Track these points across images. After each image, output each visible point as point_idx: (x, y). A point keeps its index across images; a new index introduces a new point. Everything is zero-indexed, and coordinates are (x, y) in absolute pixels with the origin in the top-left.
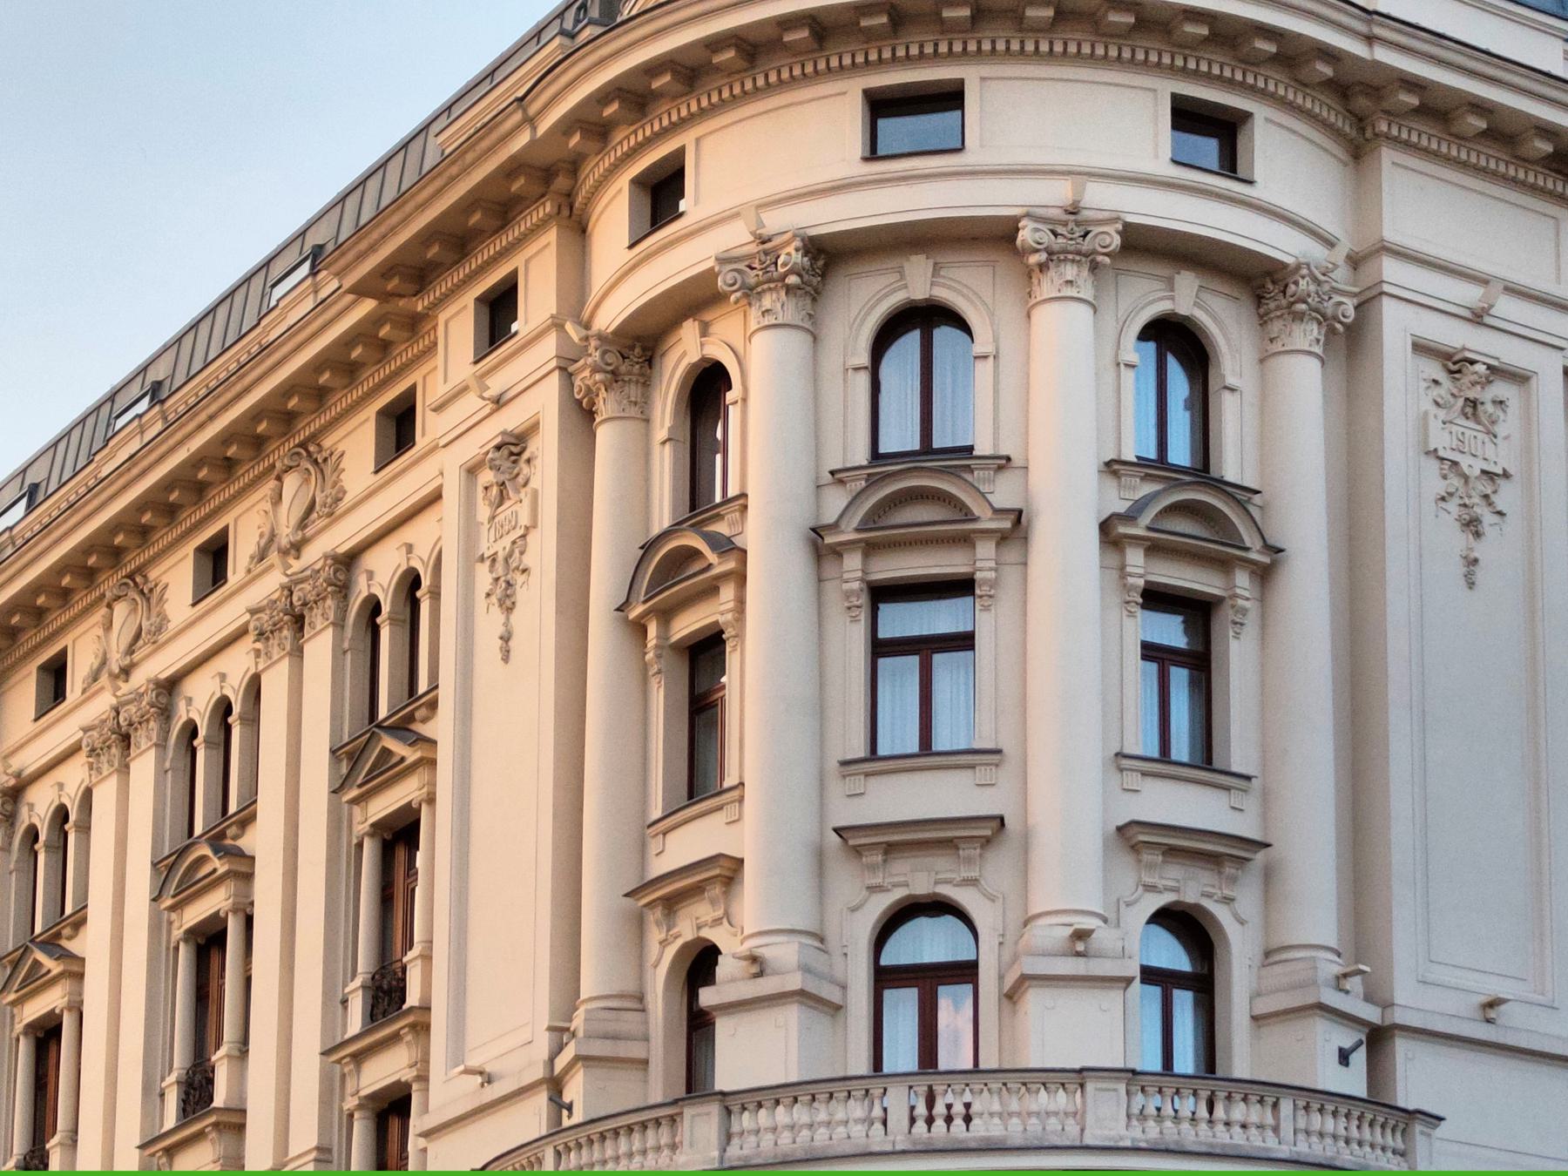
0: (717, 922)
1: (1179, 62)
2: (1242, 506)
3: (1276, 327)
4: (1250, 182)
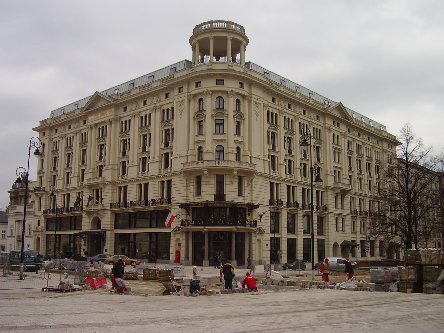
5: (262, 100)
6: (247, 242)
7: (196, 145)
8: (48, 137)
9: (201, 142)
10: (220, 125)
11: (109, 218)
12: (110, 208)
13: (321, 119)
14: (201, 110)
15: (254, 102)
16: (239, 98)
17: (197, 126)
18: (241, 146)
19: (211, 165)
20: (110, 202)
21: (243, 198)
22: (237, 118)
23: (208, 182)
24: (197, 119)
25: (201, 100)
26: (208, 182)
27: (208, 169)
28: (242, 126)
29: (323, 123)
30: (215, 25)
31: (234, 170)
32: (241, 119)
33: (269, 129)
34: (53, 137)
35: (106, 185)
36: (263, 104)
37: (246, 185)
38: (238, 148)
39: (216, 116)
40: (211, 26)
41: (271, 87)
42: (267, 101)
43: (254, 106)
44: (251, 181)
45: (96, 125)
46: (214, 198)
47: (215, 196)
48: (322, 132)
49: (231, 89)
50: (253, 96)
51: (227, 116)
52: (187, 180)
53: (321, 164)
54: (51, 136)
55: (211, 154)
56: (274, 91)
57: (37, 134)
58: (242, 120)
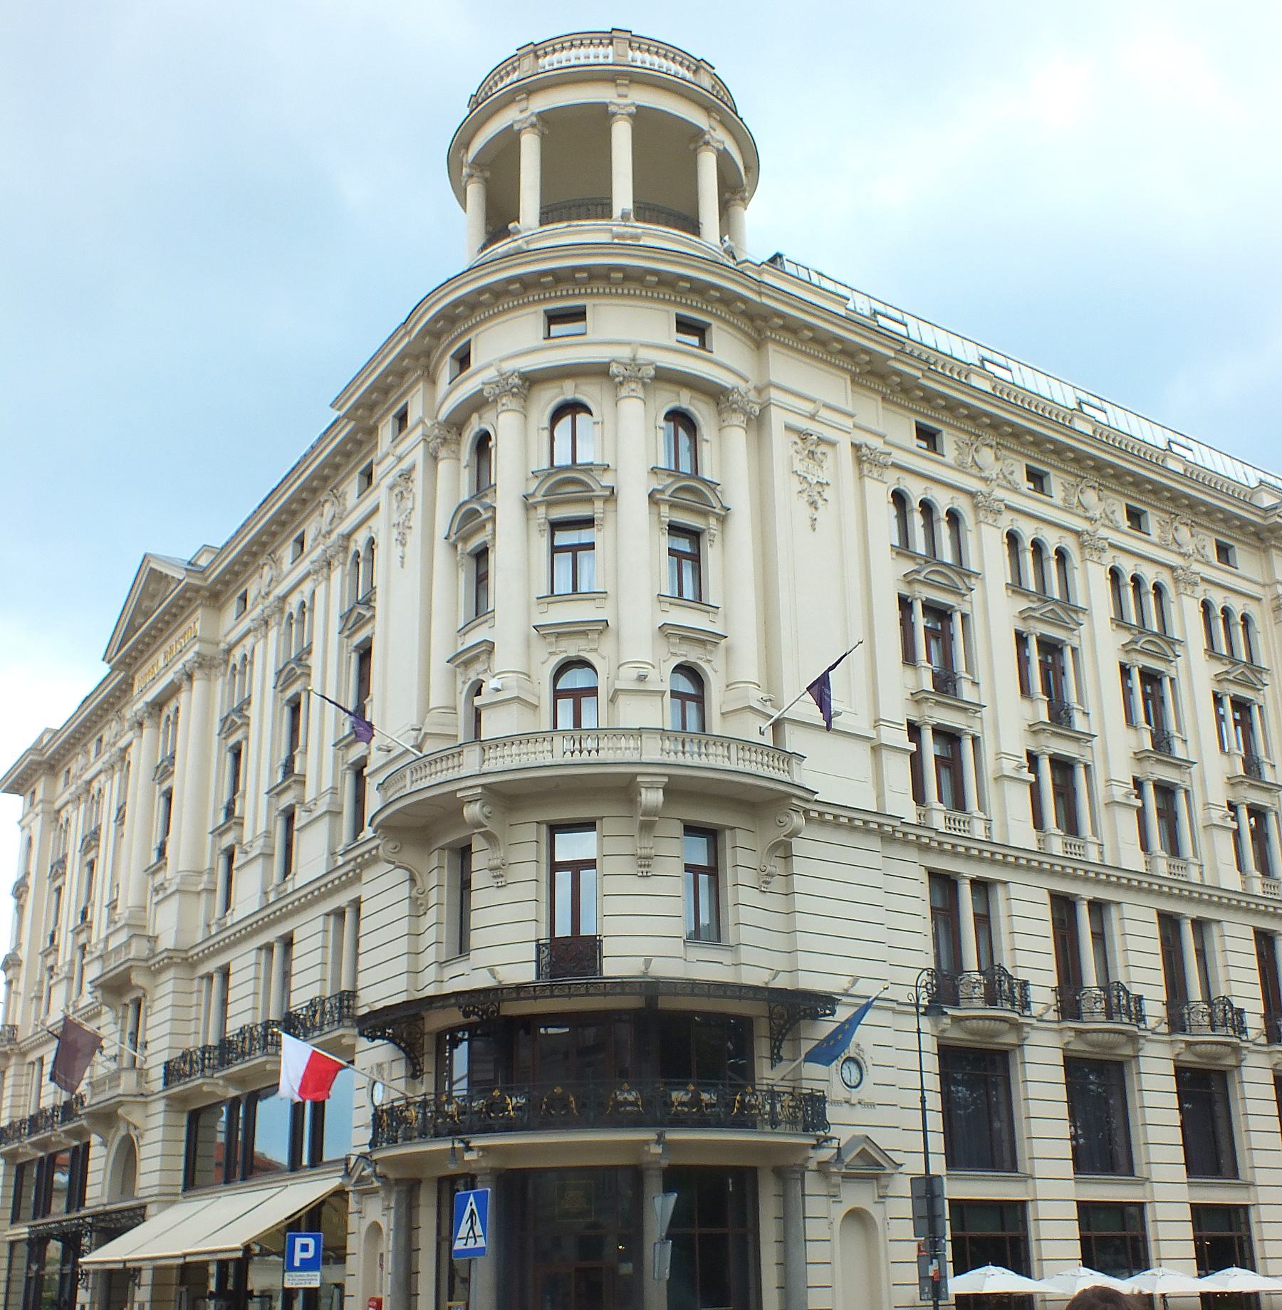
0: (485, 671)
1: (678, 299)
2: (713, 490)
3: (725, 415)
4: (711, 352)
5: (848, 423)
6: (769, 1231)
7: (460, 679)
8: (39, 808)
9: (476, 658)
10: (580, 554)
11: (158, 1134)
12: (158, 1085)
13: (1241, 555)
15: (788, 428)
16: (685, 400)
17: (464, 578)
18: (709, 661)
19: (500, 767)
20: (165, 1057)
21: (726, 957)
22: (673, 506)
23: (497, 871)
24: (465, 539)
25: (483, 443)
26: (497, 871)
27: (483, 786)
28: (711, 555)
29: (1260, 580)
31: (639, 779)
32: (705, 514)
33: (909, 583)
34: (57, 805)
35: (160, 971)
36: (856, 447)
37: (745, 876)
38: (688, 670)
39: (549, 504)
41: (892, 354)
42: (882, 436)
43: (792, 452)
44: (788, 857)
45: (157, 706)
46: (537, 961)
47: (538, 952)
48: (1257, 624)
49: (624, 353)
50: (775, 394)
51: (611, 496)
52: (412, 880)
53: (1270, 788)
54: (53, 803)
55: (515, 707)
56: (923, 388)
57: (15, 804)
58: (713, 521)
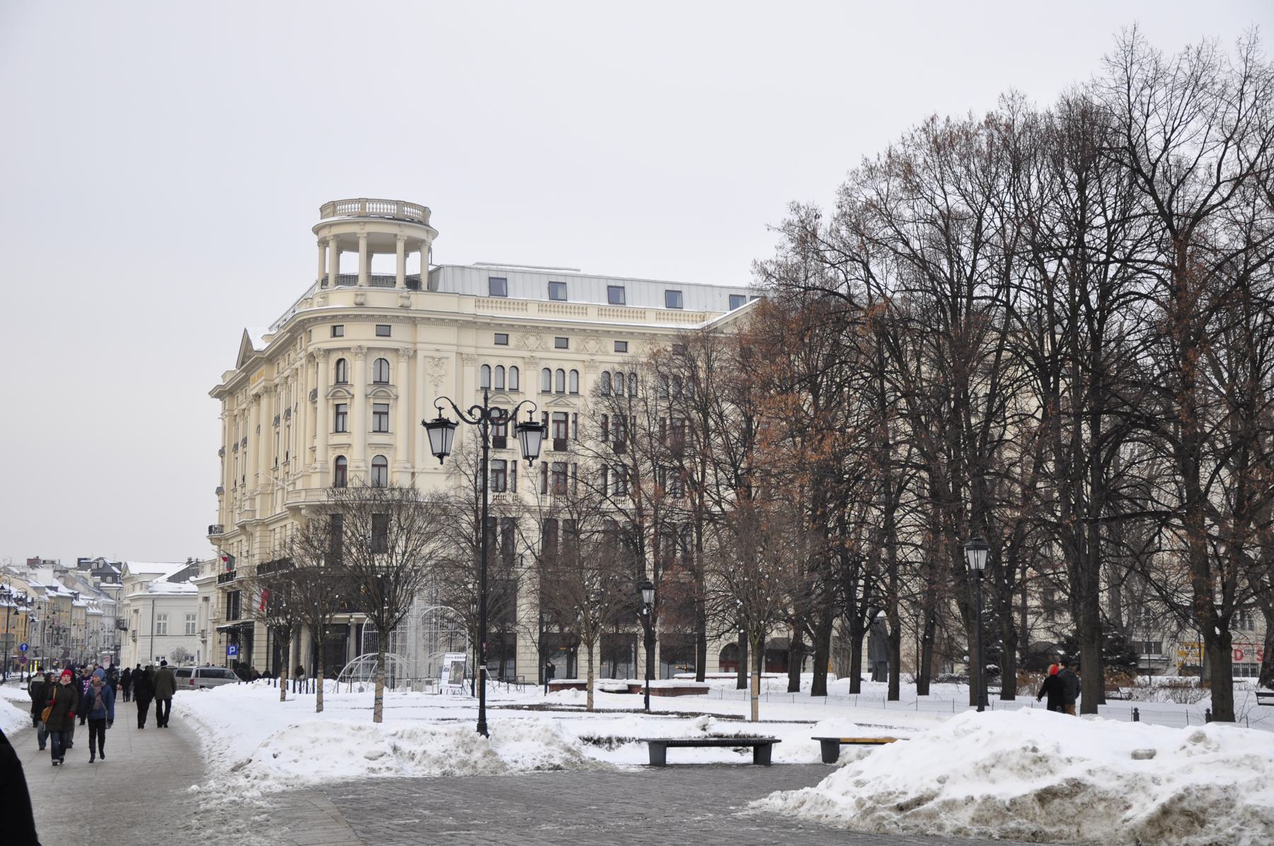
14: (341, 382)
17: (332, 413)
30: (370, 208)
40: (363, 208)
51: (397, 398)
